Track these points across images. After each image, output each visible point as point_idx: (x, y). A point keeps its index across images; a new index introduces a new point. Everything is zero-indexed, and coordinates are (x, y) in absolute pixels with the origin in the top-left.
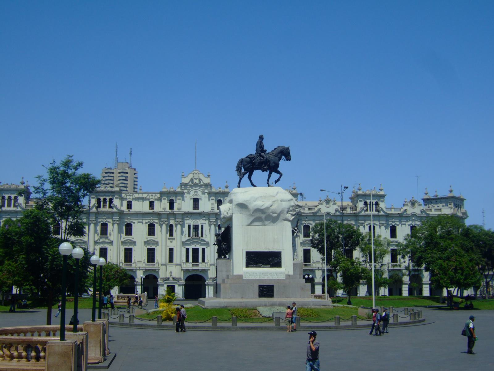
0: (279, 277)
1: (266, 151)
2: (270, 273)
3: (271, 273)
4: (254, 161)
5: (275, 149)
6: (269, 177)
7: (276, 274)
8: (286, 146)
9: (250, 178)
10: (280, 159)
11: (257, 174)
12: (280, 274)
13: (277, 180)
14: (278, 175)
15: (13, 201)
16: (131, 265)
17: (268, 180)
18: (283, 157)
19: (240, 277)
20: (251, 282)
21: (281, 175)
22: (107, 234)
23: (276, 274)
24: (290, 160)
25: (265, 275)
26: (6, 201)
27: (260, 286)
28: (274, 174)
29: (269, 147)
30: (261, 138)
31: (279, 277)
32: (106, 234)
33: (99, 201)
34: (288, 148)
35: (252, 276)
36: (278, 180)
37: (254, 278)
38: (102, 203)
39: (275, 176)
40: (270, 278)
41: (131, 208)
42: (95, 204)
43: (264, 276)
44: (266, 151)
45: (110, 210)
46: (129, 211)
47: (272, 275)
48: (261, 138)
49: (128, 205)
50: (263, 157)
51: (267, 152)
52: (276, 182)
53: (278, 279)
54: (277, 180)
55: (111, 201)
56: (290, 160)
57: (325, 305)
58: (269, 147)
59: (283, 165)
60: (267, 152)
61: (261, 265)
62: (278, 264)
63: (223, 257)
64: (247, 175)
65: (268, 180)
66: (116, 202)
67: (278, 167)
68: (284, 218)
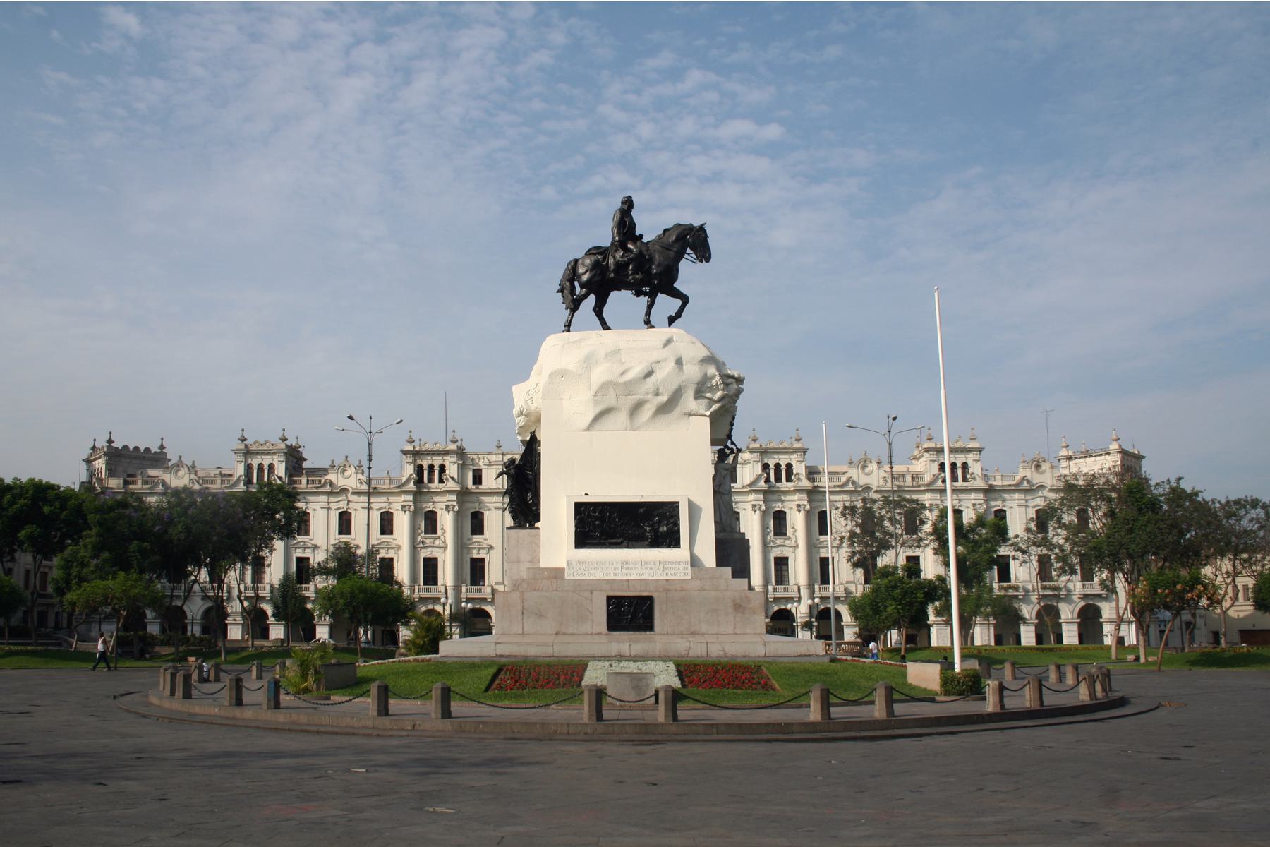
0: (671, 574)
1: (641, 236)
2: (644, 563)
3: (646, 563)
4: (605, 263)
5: (666, 231)
6: (650, 306)
7: (662, 565)
8: (696, 224)
9: (598, 310)
10: (680, 255)
11: (622, 302)
12: (674, 566)
13: (674, 315)
14: (678, 302)
15: (266, 472)
16: (483, 591)
17: (648, 314)
18: (689, 251)
19: (557, 573)
20: (590, 587)
21: (685, 300)
22: (436, 533)
23: (662, 565)
24: (708, 260)
25: (632, 569)
26: (255, 472)
27: (610, 599)
28: (661, 298)
29: (649, 226)
30: (628, 204)
31: (671, 574)
32: (435, 532)
33: (419, 470)
34: (701, 229)
35: (592, 572)
36: (679, 314)
37: (598, 578)
38: (426, 474)
39: (666, 304)
40: (643, 577)
41: (480, 483)
42: (412, 475)
43: (627, 571)
44: (641, 236)
45: (441, 485)
46: (478, 488)
47: (651, 569)
48: (628, 204)
49: (480, 477)
50: (630, 251)
51: (645, 240)
52: (672, 320)
53: (667, 580)
54: (674, 315)
55: (442, 469)
56: (708, 260)
57: (807, 654)
58: (649, 226)
59: (689, 272)
60: (645, 240)
61: (619, 541)
62: (671, 540)
63: (528, 525)
64: (592, 299)
65: (648, 314)
66: (452, 470)
67: (675, 279)
68: (687, 410)
